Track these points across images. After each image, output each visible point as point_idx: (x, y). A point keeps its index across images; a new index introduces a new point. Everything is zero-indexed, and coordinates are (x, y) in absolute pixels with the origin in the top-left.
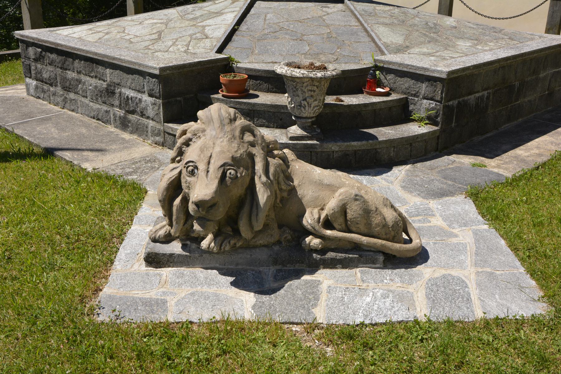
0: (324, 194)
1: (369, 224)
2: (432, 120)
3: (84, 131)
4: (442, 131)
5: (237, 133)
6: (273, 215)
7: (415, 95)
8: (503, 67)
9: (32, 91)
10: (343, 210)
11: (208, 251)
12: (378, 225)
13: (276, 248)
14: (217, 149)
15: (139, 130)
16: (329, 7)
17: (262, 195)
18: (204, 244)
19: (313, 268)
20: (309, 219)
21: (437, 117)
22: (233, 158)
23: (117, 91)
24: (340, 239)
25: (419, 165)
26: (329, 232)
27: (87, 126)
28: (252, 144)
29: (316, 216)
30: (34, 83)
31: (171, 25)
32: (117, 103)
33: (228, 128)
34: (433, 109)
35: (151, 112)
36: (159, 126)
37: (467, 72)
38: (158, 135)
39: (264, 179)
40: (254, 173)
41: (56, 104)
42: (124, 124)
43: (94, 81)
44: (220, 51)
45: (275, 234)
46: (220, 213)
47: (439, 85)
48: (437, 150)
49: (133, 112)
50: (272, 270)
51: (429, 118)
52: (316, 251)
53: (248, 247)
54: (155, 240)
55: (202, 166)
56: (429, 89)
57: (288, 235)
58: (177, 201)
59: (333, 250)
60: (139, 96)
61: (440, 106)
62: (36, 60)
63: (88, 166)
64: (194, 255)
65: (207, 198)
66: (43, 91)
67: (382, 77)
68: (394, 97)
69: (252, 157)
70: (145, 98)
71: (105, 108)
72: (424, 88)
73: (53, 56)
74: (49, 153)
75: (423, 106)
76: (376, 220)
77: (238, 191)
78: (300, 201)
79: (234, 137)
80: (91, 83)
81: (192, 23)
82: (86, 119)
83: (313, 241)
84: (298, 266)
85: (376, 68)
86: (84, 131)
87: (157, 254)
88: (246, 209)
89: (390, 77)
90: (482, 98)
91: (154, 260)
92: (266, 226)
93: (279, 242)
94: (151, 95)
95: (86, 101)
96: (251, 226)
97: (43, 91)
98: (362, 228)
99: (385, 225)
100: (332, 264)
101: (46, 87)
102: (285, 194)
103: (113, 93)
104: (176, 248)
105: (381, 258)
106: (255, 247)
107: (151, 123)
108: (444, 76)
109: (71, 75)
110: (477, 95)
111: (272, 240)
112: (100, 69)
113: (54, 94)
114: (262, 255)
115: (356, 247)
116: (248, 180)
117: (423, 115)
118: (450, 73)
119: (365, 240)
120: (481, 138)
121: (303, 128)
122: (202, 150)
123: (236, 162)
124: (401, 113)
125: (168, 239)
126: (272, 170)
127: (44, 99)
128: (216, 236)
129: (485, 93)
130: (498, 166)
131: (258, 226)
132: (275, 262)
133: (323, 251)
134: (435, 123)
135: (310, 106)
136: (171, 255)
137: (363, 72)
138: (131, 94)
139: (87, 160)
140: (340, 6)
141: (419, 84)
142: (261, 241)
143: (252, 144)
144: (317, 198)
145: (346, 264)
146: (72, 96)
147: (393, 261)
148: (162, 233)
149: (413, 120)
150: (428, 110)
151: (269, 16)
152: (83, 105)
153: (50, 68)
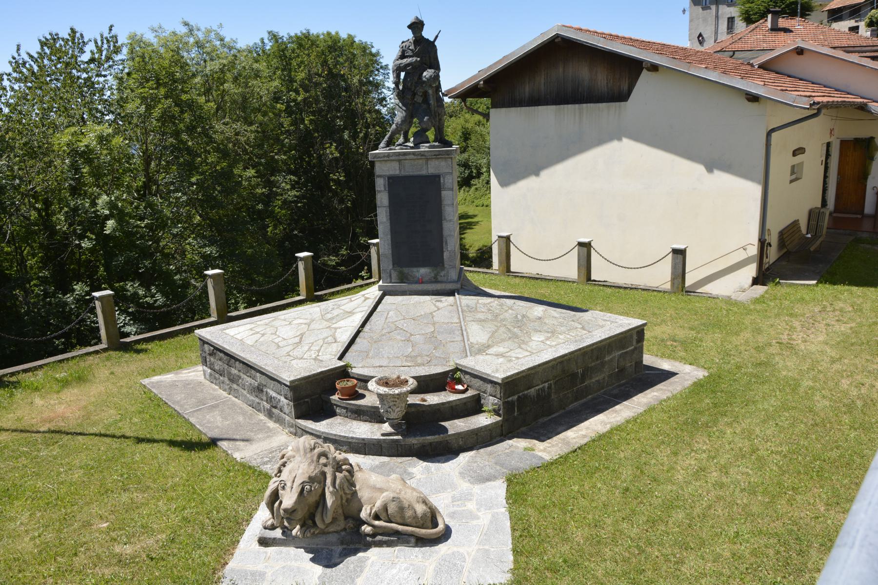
0: (375, 495)
1: (403, 517)
2: (496, 412)
3: (241, 419)
4: (503, 421)
5: (315, 458)
6: (340, 511)
7: (484, 392)
8: (561, 362)
9: (207, 376)
10: (385, 508)
11: (296, 537)
12: (409, 517)
13: (343, 533)
14: (300, 471)
15: (279, 421)
16: (441, 301)
17: (330, 500)
18: (294, 532)
19: (367, 547)
20: (363, 515)
21: (499, 410)
22: (310, 478)
23: (265, 390)
24: (385, 528)
25: (482, 450)
26: (377, 523)
27: (244, 413)
28: (325, 465)
29: (368, 512)
30: (209, 371)
31: (312, 326)
32: (265, 398)
33: (309, 455)
34: (496, 404)
35: (286, 410)
36: (292, 421)
37: (524, 374)
38: (292, 427)
39: (331, 489)
40: (325, 485)
41: (225, 390)
42: (270, 415)
43: (249, 379)
44: (341, 358)
45: (342, 524)
46: (299, 515)
47: (498, 387)
48: (502, 435)
49: (275, 407)
50: (340, 548)
51: (494, 410)
52: (368, 535)
53: (323, 533)
54: (265, 528)
55: (289, 484)
56: (493, 389)
57: (351, 524)
58: (277, 503)
59: (381, 534)
60: (279, 397)
61: (501, 403)
62: (210, 355)
63: (237, 456)
64: (287, 540)
65: (289, 507)
66: (215, 378)
67: (462, 377)
68: (470, 393)
69: (324, 474)
70: (282, 399)
71: (257, 400)
72: (489, 388)
73: (222, 355)
74: (213, 443)
75: (490, 402)
76: (408, 513)
77: (312, 499)
78: (359, 501)
79: (312, 461)
80: (248, 380)
81: (328, 324)
82: (245, 406)
83: (366, 529)
84: (357, 546)
85: (457, 370)
86: (241, 419)
87: (265, 538)
88: (320, 509)
89: (467, 377)
90: (543, 389)
91: (264, 542)
92: (334, 519)
93: (345, 529)
94: (286, 398)
95: (245, 392)
96: (323, 521)
97: (215, 378)
98: (399, 520)
99: (415, 517)
100: (380, 544)
101: (217, 376)
102: (349, 496)
103: (262, 391)
104: (278, 533)
105: (413, 540)
106: (329, 533)
107: (287, 418)
108: (500, 381)
109: (234, 371)
110: (537, 388)
111: (339, 528)
112: (253, 372)
113: (223, 383)
114: (333, 538)
115: (397, 533)
116: (320, 491)
117: (491, 408)
118: (503, 379)
119: (400, 528)
120: (546, 419)
121: (392, 426)
122: (290, 472)
123: (312, 480)
124: (474, 407)
125: (273, 528)
126: (338, 482)
127: (216, 384)
128: (302, 527)
129: (546, 385)
130: (544, 450)
131: (328, 520)
132: (342, 543)
133: (374, 535)
134: (499, 415)
135: (394, 411)
136: (274, 539)
137: (445, 374)
138: (274, 394)
139: (238, 450)
140: (451, 298)
141: (486, 385)
142: (332, 529)
143: (325, 465)
144: (371, 498)
145: (389, 544)
146: (235, 386)
147: (422, 542)
148: (269, 523)
149: (484, 411)
150: (493, 405)
151: (391, 313)
152: (243, 395)
153: (220, 363)
